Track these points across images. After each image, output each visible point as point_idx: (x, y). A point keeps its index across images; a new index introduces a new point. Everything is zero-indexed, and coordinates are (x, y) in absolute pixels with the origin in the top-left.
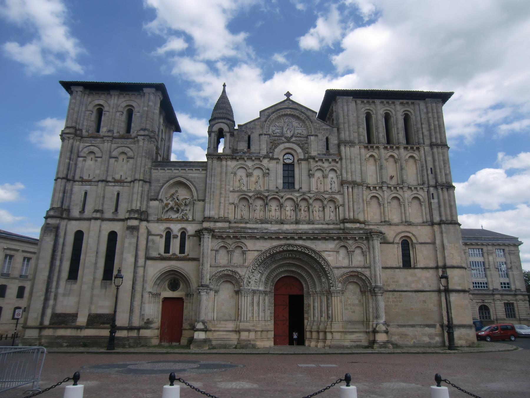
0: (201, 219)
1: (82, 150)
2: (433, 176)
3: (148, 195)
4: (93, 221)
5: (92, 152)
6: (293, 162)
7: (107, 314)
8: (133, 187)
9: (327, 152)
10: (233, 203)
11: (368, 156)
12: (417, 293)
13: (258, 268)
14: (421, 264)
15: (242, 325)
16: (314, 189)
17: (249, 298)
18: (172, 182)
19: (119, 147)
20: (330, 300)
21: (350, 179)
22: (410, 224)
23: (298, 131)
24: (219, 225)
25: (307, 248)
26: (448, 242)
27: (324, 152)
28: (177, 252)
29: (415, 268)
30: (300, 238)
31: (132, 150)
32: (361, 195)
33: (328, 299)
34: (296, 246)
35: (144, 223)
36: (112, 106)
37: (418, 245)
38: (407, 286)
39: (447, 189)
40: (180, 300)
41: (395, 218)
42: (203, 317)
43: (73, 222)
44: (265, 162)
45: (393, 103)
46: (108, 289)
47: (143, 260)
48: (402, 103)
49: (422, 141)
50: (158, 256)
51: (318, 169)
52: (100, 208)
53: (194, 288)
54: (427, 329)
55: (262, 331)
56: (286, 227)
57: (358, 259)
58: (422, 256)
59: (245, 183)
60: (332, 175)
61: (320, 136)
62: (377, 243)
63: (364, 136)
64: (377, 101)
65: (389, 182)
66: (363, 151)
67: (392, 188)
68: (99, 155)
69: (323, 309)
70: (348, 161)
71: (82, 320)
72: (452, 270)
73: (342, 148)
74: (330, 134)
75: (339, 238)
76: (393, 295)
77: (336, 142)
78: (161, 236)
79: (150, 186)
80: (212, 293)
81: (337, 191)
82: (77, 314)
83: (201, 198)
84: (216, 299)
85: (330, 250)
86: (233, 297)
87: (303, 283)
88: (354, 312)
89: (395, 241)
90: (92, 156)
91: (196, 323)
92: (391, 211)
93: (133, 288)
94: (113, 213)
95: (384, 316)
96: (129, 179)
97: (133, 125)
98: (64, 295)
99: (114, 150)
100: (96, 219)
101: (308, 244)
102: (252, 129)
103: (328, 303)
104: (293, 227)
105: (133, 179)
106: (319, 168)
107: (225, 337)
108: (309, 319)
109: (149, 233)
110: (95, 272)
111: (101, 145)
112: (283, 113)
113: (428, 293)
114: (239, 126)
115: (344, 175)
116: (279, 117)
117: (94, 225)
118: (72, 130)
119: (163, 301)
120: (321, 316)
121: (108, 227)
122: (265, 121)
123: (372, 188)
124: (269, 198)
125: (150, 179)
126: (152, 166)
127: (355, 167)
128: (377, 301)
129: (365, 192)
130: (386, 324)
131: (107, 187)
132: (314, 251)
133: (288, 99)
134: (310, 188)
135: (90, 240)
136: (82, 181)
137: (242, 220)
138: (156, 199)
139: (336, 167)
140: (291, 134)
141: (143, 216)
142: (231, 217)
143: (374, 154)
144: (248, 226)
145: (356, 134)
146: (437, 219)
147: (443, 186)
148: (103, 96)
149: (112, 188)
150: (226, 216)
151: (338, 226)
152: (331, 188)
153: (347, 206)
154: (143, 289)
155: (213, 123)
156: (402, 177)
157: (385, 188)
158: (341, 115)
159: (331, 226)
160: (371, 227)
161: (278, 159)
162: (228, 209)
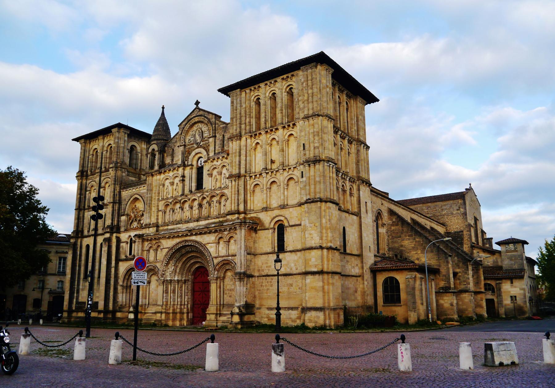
18: (132, 199)
22: (283, 207)
25: (196, 242)
30: (192, 235)
37: (290, 228)
43: (85, 239)
48: (283, 79)
67: (270, 173)
72: (310, 251)
75: (216, 231)
76: (266, 279)
78: (127, 243)
85: (211, 242)
88: (230, 296)
92: (270, 196)
101: (198, 238)
107: (150, 317)
112: (194, 121)
122: (181, 134)
124: (182, 201)
126: (120, 189)
132: (200, 244)
138: (123, 215)
144: (169, 227)
147: (309, 162)
157: (264, 175)
162: (158, 216)
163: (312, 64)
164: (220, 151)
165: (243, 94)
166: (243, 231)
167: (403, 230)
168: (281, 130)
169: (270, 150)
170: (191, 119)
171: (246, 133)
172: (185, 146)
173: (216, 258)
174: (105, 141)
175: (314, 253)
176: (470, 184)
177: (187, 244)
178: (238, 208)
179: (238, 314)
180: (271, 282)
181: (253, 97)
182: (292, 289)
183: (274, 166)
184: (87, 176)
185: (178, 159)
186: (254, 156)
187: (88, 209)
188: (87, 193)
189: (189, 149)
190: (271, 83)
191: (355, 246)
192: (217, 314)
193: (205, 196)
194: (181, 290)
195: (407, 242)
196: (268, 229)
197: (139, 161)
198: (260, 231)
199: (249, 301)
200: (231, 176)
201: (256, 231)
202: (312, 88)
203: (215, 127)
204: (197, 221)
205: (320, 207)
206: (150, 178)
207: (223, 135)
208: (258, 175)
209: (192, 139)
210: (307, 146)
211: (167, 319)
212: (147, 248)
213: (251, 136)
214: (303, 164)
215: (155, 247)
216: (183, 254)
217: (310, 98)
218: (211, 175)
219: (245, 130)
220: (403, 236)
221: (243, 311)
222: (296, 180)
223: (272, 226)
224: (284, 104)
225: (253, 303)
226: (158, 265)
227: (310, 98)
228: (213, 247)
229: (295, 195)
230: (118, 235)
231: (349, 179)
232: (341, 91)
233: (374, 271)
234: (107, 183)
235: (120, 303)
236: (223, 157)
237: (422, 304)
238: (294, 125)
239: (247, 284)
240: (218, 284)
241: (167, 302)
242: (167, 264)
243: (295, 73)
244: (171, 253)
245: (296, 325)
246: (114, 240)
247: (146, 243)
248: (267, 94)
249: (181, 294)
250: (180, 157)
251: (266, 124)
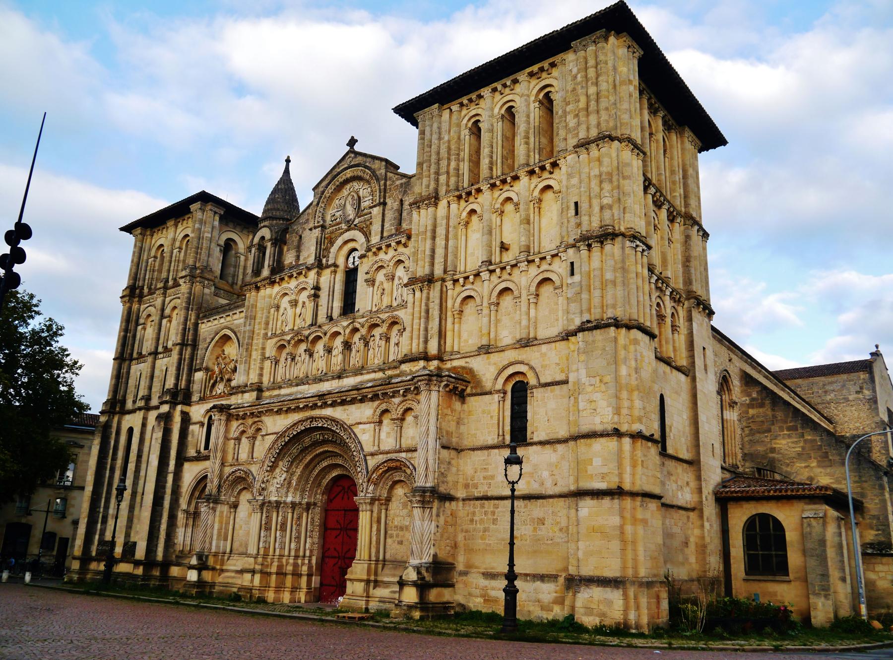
12: (526, 502)
18: (217, 338)
22: (526, 343)
25: (333, 420)
29: (532, 444)
30: (325, 405)
37: (541, 390)
39: (602, 243)
43: (127, 417)
48: (531, 75)
50: (195, 455)
67: (498, 270)
72: (589, 441)
75: (375, 397)
78: (202, 424)
85: (365, 420)
88: (401, 543)
92: (497, 321)
101: (337, 413)
107: (230, 581)
112: (344, 178)
113: (551, 500)
122: (318, 204)
124: (311, 338)
126: (198, 317)
133: (352, 151)
138: (200, 370)
147: (588, 238)
157: (485, 275)
162: (262, 369)
163: (598, 33)
164: (393, 231)
165: (446, 114)
166: (434, 395)
167: (774, 416)
168: (524, 180)
169: (499, 223)
170: (339, 173)
171: (447, 192)
172: (323, 227)
173: (372, 454)
174: (179, 231)
175: (599, 445)
176: (877, 347)
177: (315, 424)
178: (426, 348)
179: (414, 584)
180: (493, 513)
181: (467, 118)
182: (543, 532)
183: (508, 257)
184: (141, 296)
185: (309, 255)
186: (464, 238)
187: (137, 359)
188: (140, 327)
189: (332, 233)
190: (505, 86)
191: (683, 440)
192: (368, 582)
193: (358, 326)
194: (299, 525)
195: (784, 442)
196: (490, 393)
197: (241, 271)
198: (472, 398)
199: (443, 555)
200: (412, 281)
201: (462, 397)
202: (597, 84)
203: (385, 185)
204: (339, 377)
205: (616, 340)
206: (254, 293)
207: (401, 200)
208: (471, 277)
209: (338, 214)
210: (583, 207)
211: (265, 586)
212: (236, 434)
213: (459, 197)
214: (574, 246)
215: (251, 432)
216: (306, 448)
217: (593, 104)
218: (371, 282)
219: (448, 185)
220: (775, 428)
221: (428, 577)
222: (558, 283)
223: (499, 385)
224: (532, 126)
225: (450, 560)
226: (254, 469)
227: (593, 104)
228: (369, 432)
229: (553, 314)
230: (186, 409)
231: (671, 293)
232: (653, 111)
233: (724, 501)
234: (175, 308)
235: (179, 548)
236: (399, 243)
237: (843, 580)
238: (555, 165)
239: (438, 515)
240: (375, 515)
241: (267, 549)
242: (273, 468)
243: (557, 59)
244: (281, 443)
245: (550, 618)
247: (235, 424)
248: (496, 110)
249: (299, 532)
251: (491, 169)
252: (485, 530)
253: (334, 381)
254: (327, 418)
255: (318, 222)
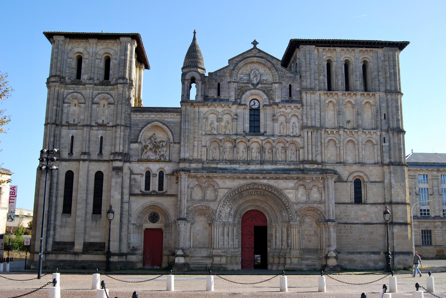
0: (177, 161)
1: (66, 97)
2: (386, 121)
3: (129, 139)
4: (81, 162)
5: (76, 98)
6: (259, 107)
7: (99, 243)
8: (116, 132)
9: (290, 99)
10: (205, 146)
11: (327, 102)
12: (365, 226)
13: (228, 203)
14: (370, 201)
15: (215, 252)
16: (277, 133)
17: (221, 229)
19: (99, 94)
20: (290, 231)
21: (309, 125)
22: (362, 164)
23: (264, 78)
24: (194, 165)
26: (395, 182)
27: (287, 99)
28: (157, 189)
29: (365, 204)
31: (112, 96)
32: (319, 139)
33: (288, 230)
34: (261, 184)
35: (127, 164)
36: (91, 54)
37: (369, 184)
38: (357, 219)
40: (160, 231)
41: (350, 159)
42: (182, 245)
43: (64, 163)
44: (234, 107)
45: (354, 50)
46: (98, 222)
47: (128, 196)
49: (377, 88)
50: (140, 193)
51: (281, 115)
52: (87, 151)
53: (172, 221)
54: (372, 255)
55: (232, 257)
56: (252, 167)
57: (315, 195)
58: (372, 193)
59: (215, 127)
60: (294, 120)
61: (284, 83)
62: (331, 183)
63: (324, 83)
64: (338, 49)
65: (345, 127)
66: (323, 97)
67: (348, 132)
68: (83, 101)
69: (284, 239)
70: (309, 108)
71: (78, 247)
72: (396, 205)
73: (304, 95)
74: (293, 82)
75: (298, 178)
76: (345, 227)
77: (298, 89)
79: (130, 130)
80: (189, 225)
81: (298, 135)
82: (74, 242)
83: (177, 140)
84: (192, 230)
86: (206, 228)
87: (267, 216)
88: (310, 241)
89: (349, 180)
90: (76, 102)
91: (176, 250)
93: (121, 221)
94: (98, 155)
95: (335, 245)
96: (111, 124)
97: (111, 72)
98: (61, 226)
99: (95, 97)
100: (84, 160)
102: (222, 76)
103: (287, 234)
104: (258, 167)
105: (114, 124)
106: (282, 113)
107: (201, 261)
108: (272, 247)
109: (132, 173)
110: (86, 207)
111: (84, 92)
113: (376, 225)
114: (209, 73)
115: (305, 121)
116: (246, 64)
117: (84, 166)
118: (57, 79)
119: (144, 232)
120: (282, 245)
121: (95, 167)
122: (234, 69)
123: (329, 132)
125: (130, 124)
127: (315, 112)
128: (329, 232)
129: (323, 136)
130: (336, 251)
131: (92, 131)
132: (276, 189)
133: (255, 47)
134: (273, 133)
135: (80, 180)
136: (68, 126)
137: (214, 161)
138: (136, 142)
139: (298, 112)
140: (258, 82)
141: (126, 157)
142: (204, 158)
143: (333, 100)
144: (219, 166)
145: (317, 81)
146: (387, 161)
148: (82, 44)
149: (95, 132)
150: (199, 158)
151: (299, 167)
152: (293, 132)
153: (306, 149)
154: (129, 221)
155: (185, 70)
156: (357, 122)
158: (303, 64)
159: (292, 167)
160: (328, 167)
161: (245, 105)
162: (201, 151)
208: (335, 132)
217: (393, 76)
246: (126, 170)
250: (233, 93)
252: (347, 236)
253: (257, 166)
254: (265, 185)
255: (234, 79)
